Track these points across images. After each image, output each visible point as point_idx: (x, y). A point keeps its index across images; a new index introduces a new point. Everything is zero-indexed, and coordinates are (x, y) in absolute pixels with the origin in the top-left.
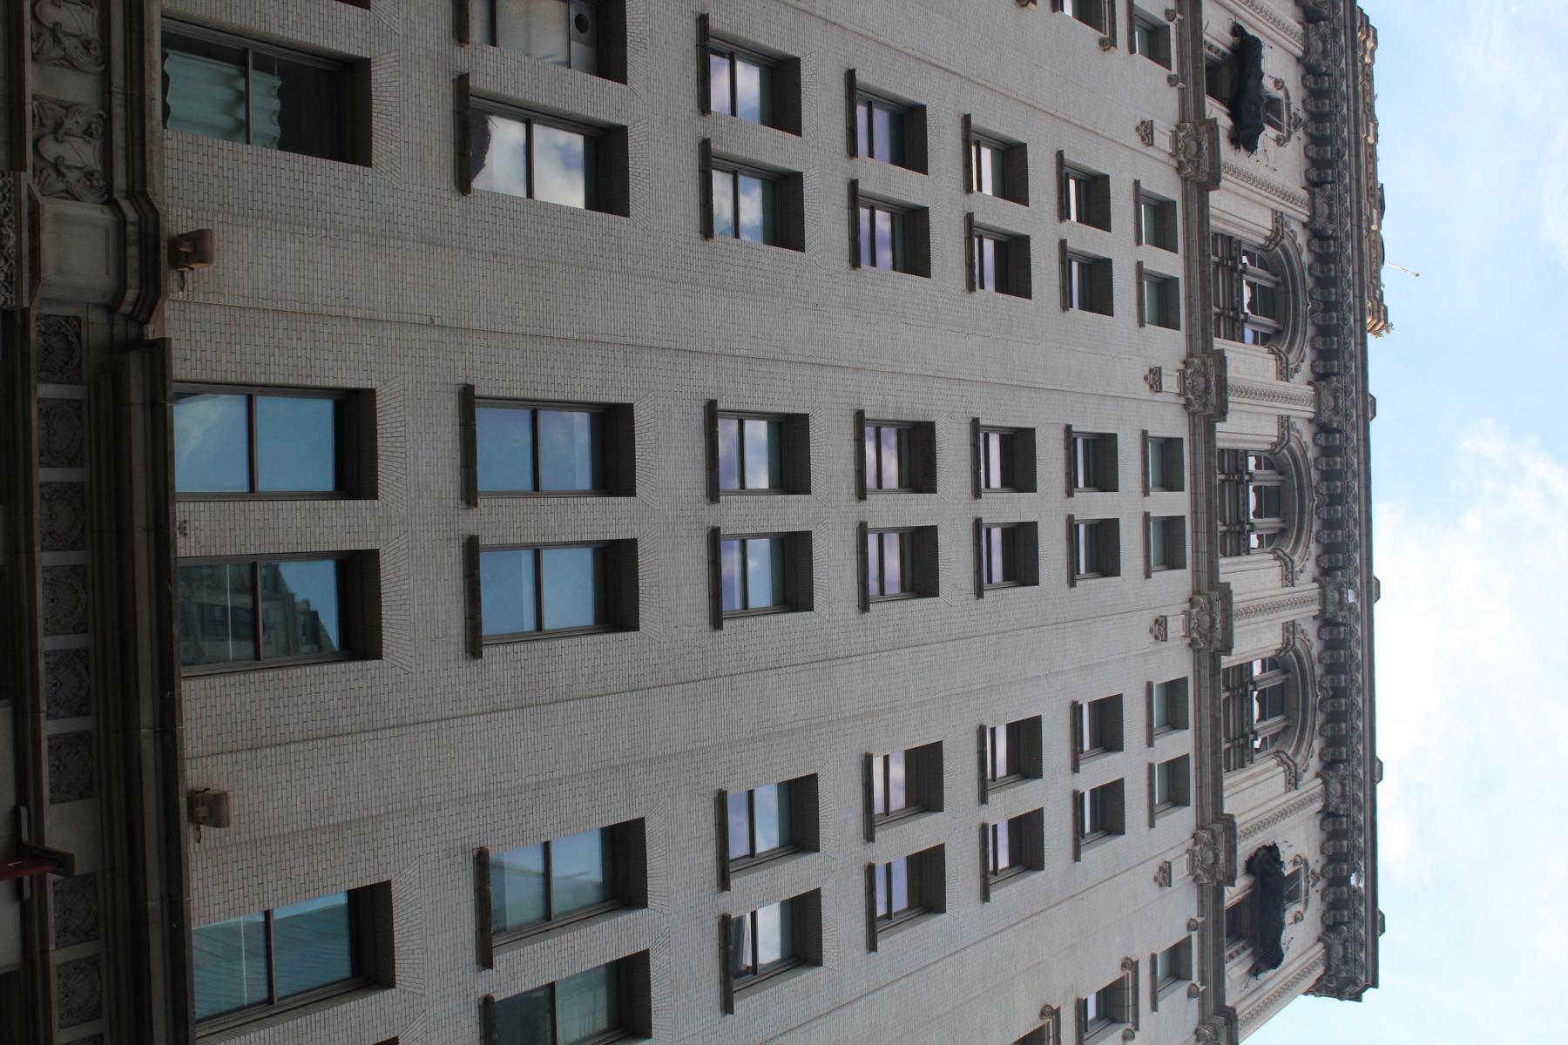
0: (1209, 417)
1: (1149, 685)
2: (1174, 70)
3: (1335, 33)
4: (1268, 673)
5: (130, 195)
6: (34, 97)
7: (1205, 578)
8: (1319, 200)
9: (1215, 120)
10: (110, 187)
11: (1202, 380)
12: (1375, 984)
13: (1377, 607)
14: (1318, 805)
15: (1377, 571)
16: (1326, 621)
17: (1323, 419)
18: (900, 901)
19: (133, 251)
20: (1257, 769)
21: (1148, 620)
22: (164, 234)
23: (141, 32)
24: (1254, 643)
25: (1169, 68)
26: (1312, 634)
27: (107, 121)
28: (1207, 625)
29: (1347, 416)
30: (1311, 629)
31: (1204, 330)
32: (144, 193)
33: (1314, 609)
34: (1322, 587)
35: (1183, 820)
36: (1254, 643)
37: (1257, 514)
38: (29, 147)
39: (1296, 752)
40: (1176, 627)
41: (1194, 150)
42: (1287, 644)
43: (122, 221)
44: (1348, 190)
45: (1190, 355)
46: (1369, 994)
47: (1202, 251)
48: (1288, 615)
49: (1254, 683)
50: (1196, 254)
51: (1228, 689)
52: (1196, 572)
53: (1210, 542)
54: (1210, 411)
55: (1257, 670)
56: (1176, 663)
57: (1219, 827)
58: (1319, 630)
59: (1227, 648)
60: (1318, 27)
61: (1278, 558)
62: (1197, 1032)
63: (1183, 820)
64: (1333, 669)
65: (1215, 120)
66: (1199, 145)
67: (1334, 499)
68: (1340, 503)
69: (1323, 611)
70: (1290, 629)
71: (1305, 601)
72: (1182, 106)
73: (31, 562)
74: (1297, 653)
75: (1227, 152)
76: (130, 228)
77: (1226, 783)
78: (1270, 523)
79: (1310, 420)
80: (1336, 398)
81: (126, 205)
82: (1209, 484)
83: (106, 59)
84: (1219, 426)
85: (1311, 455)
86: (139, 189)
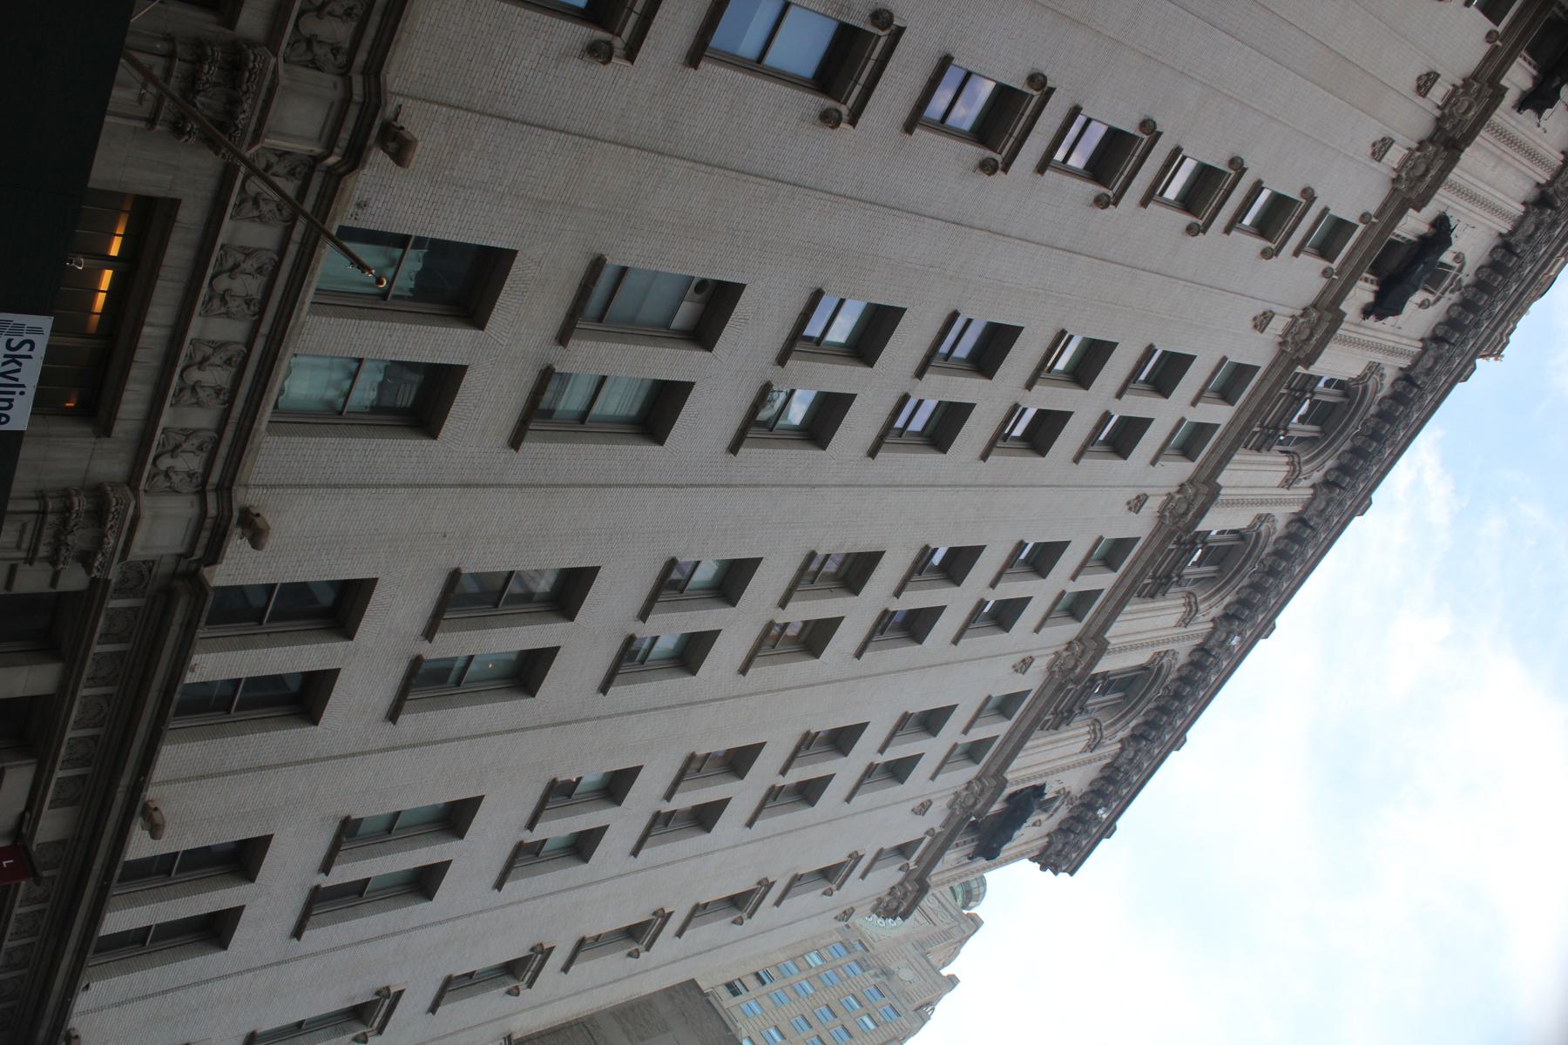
0: (1409, 200)
1: (1224, 359)
2: (1500, 29)
3: (1554, 224)
4: (1331, 390)
5: (365, 72)
6: (222, 246)
7: (1329, 298)
8: (1431, 353)
9: (1344, 314)
10: (204, 483)
11: (1184, 506)
12: (1072, 873)
13: (1104, 842)
14: (1297, 509)
15: (1279, 621)
16: (1406, 378)
17: (1513, 240)
18: (963, 351)
19: (205, 535)
20: (1269, 459)
21: (1258, 308)
22: (235, 506)
23: (265, 386)
24: (1337, 363)
25: (1497, 24)
26: (1387, 382)
27: (217, 443)
28: (1181, 511)
29: (1535, 248)
30: (1390, 374)
31: (1362, 261)
32: (229, 489)
33: (1405, 363)
34: (1425, 350)
35: (1179, 470)
36: (1337, 363)
37: (1302, 420)
38: (178, 370)
39: (1308, 462)
40: (1278, 326)
41: (1419, 172)
42: (1362, 378)
43: (347, 100)
44: (1534, 260)
45: (1314, 306)
46: (1063, 876)
47: (1144, 569)
48: (1378, 357)
49: (1313, 394)
50: (1246, 415)
51: (1288, 387)
52: (1201, 467)
53: (1281, 376)
54: (1413, 195)
55: (1321, 384)
56: (1258, 351)
57: (994, 783)
58: (1396, 380)
59: (1309, 361)
60: (1541, 213)
61: (1291, 463)
62: (970, 783)
63: (1179, 470)
64: (1384, 416)
65: (1506, 89)
66: (1311, 335)
67: (1272, 572)
68: (1378, 441)
69: (1410, 368)
70: (1374, 368)
71: (1401, 354)
72: (1323, 292)
73: (88, 647)
74: (1365, 389)
75: (1504, 115)
76: (208, 523)
77: (1236, 457)
78: (1310, 430)
79: (1538, 185)
80: (1436, 362)
81: (211, 499)
82: (1270, 391)
83: (230, 402)
84: (1411, 211)
85: (1171, 677)
86: (374, 70)
